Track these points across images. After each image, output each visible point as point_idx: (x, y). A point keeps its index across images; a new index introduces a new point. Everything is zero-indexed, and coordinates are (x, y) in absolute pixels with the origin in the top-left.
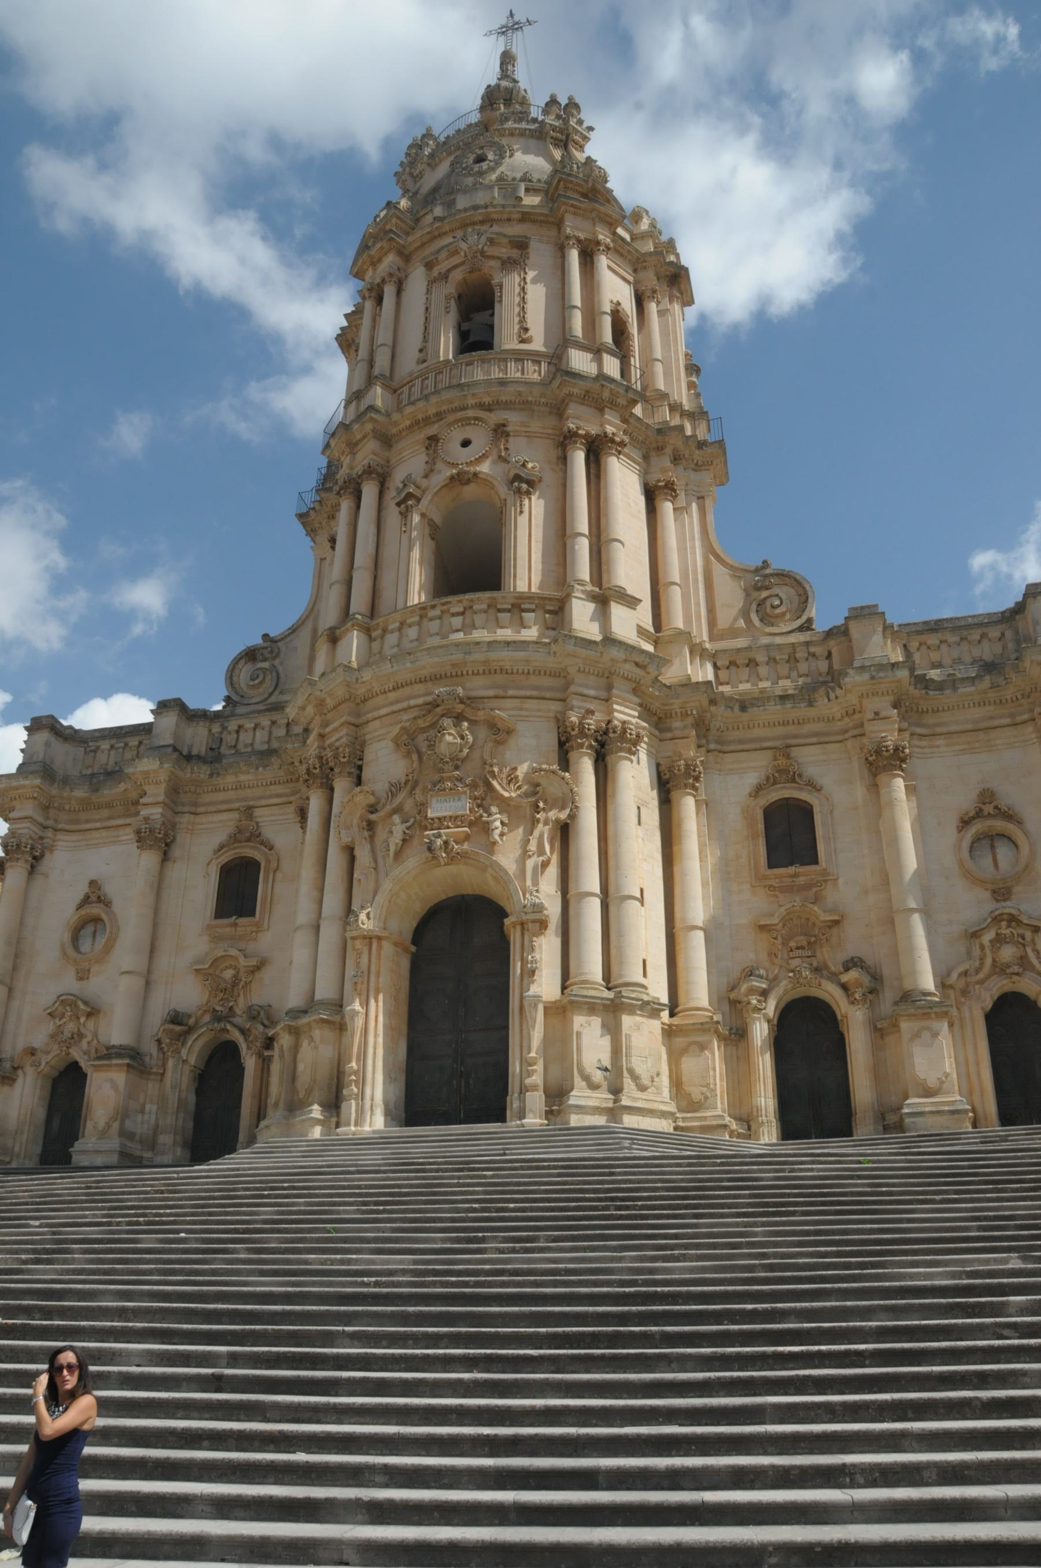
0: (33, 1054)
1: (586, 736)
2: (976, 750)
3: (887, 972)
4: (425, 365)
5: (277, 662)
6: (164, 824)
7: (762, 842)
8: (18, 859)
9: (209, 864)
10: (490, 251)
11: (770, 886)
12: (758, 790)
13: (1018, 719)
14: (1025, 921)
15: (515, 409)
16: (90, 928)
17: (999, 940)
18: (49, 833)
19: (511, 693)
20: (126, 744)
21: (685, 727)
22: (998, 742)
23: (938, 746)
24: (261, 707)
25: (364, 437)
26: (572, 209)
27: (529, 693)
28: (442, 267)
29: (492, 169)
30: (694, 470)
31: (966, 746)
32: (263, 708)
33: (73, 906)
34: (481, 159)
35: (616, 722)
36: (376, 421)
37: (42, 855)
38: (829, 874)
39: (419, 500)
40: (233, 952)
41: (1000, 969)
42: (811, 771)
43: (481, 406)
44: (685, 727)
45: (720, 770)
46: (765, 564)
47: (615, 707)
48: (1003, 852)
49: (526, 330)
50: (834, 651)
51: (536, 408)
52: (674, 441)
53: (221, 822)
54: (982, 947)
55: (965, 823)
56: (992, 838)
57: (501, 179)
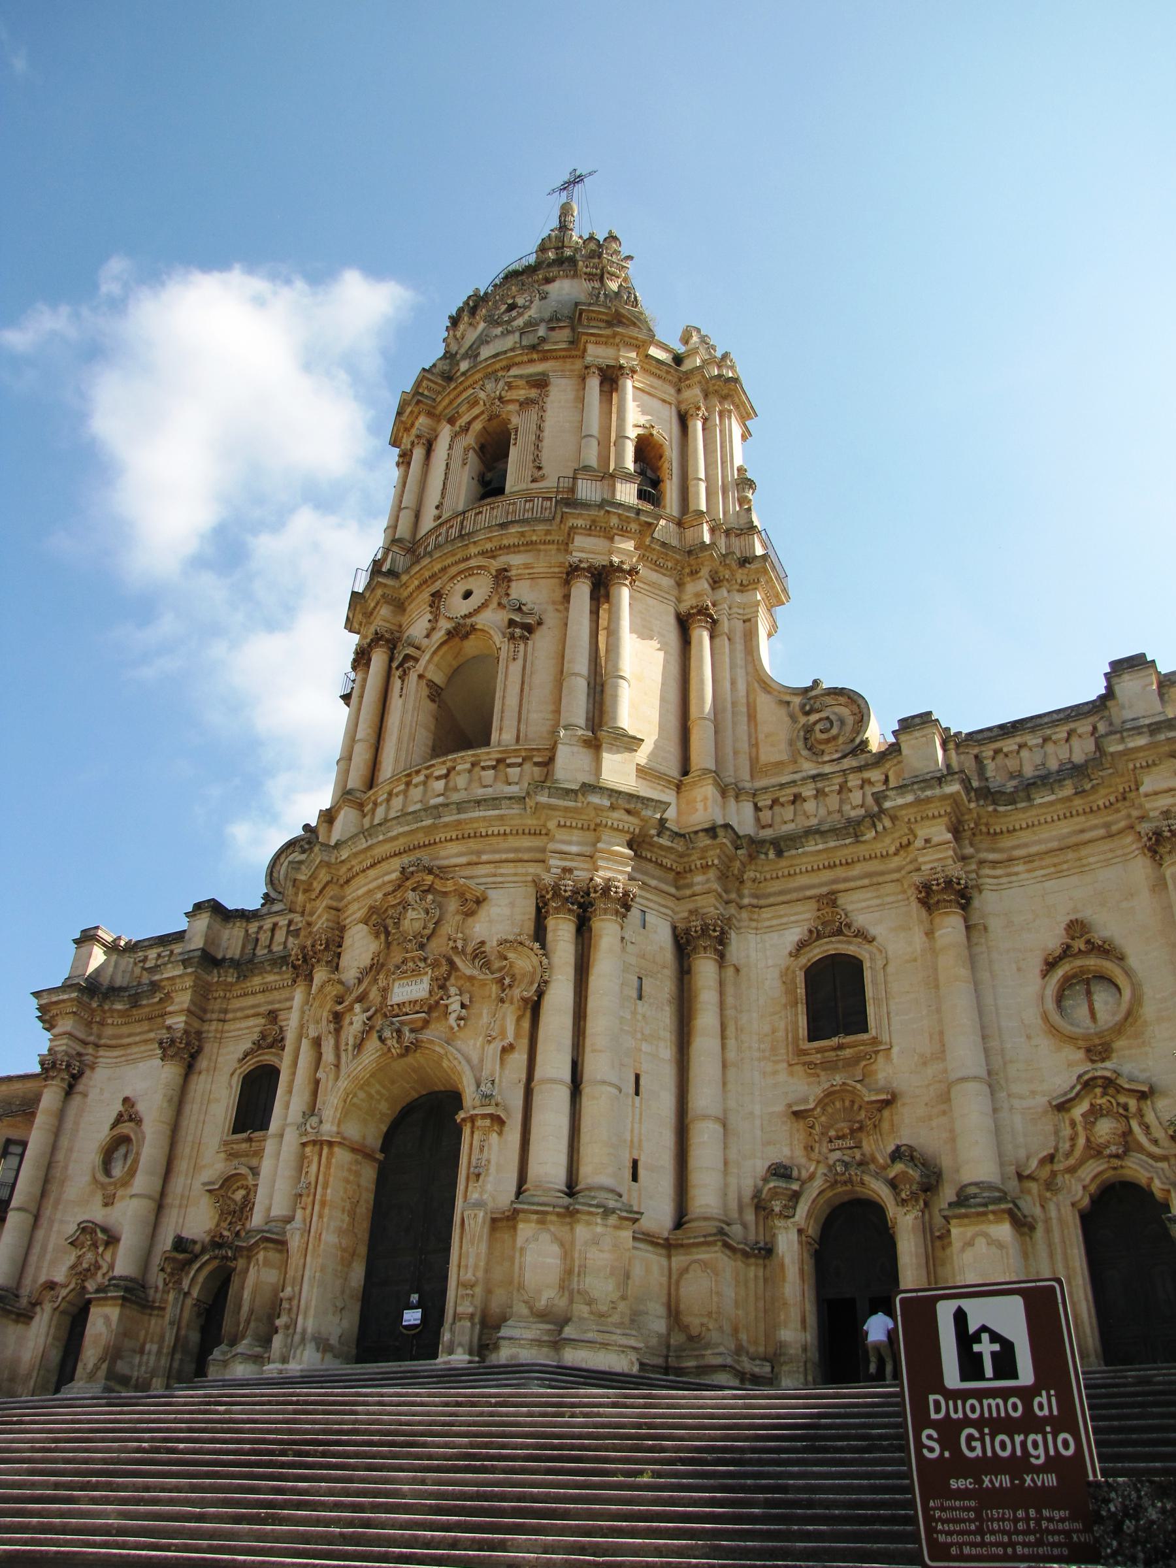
0: (52, 1289)
2: (1065, 873)
3: (946, 1162)
6: (186, 1032)
7: (802, 1009)
8: (53, 1078)
9: (232, 1074)
10: (509, 396)
11: (811, 1063)
12: (801, 946)
13: (1114, 828)
14: (1126, 1086)
15: (519, 552)
16: (122, 1150)
17: (1095, 1113)
18: (90, 1050)
19: (484, 858)
20: (172, 952)
21: (708, 881)
22: (1091, 860)
23: (1017, 874)
25: (377, 604)
26: (593, 339)
27: (504, 856)
28: (462, 421)
30: (739, 591)
31: (1052, 870)
33: (108, 1126)
34: (512, 307)
35: (599, 880)
36: (385, 585)
37: (81, 1073)
38: (881, 1043)
39: (417, 660)
40: (244, 1170)
41: (1094, 1151)
42: (861, 920)
43: (483, 553)
44: (708, 881)
45: (757, 929)
46: (816, 683)
48: (1102, 998)
49: (540, 468)
50: (891, 774)
51: (542, 547)
53: (248, 1028)
54: (1073, 1124)
55: (1051, 965)
56: (1087, 981)
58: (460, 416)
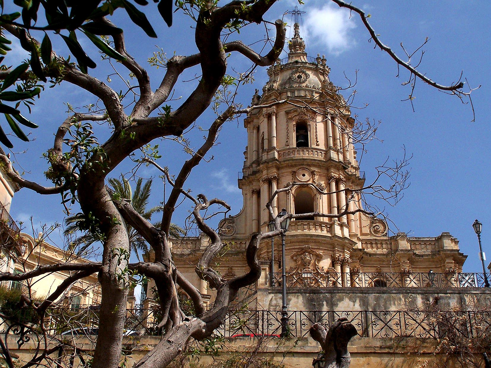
1: (339, 261)
4: (288, 147)
5: (234, 224)
15: (316, 167)
19: (321, 248)
24: (231, 237)
29: (304, 82)
32: (232, 238)
47: (345, 254)
52: (353, 178)
57: (307, 86)
58: (291, 113)
